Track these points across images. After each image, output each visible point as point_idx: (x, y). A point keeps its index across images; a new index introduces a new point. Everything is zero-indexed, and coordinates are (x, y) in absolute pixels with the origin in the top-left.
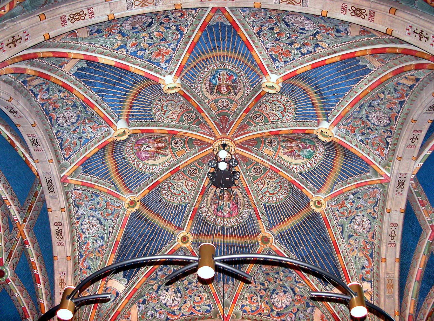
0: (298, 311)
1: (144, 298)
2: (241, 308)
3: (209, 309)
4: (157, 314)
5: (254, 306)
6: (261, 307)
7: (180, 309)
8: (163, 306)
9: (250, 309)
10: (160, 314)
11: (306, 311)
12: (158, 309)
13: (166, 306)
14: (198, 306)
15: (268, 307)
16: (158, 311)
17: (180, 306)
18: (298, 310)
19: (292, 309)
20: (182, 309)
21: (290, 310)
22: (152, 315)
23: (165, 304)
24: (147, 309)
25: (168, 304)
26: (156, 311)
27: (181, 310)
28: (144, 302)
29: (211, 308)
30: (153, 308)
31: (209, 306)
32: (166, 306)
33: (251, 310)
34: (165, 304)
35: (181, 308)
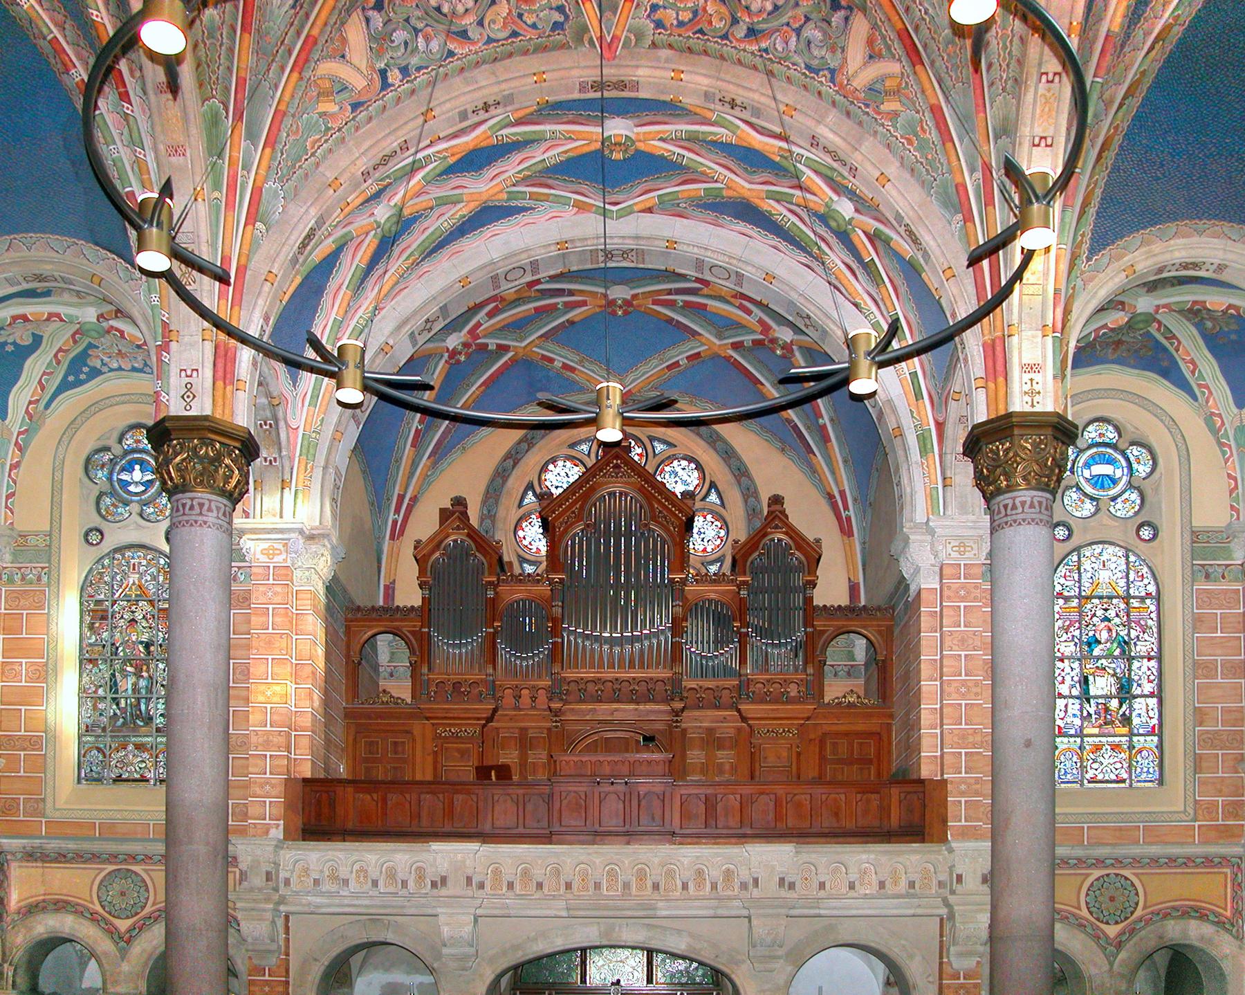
0: (805, 23)
2: (649, 16)
3: (562, 19)
4: (419, 40)
5: (685, 9)
6: (704, 10)
7: (480, 23)
8: (434, 14)
9: (675, 15)
10: (427, 39)
11: (829, 23)
12: (420, 25)
13: (441, 13)
14: (530, 12)
15: (723, 9)
16: (421, 30)
17: (479, 13)
18: (807, 19)
19: (790, 18)
20: (486, 23)
21: (784, 20)
22: (406, 43)
23: (438, 9)
24: (391, 27)
26: (416, 31)
27: (482, 26)
29: (567, 17)
30: (407, 20)
31: (560, 9)
32: (441, 13)
33: (677, 19)
35: (482, 18)
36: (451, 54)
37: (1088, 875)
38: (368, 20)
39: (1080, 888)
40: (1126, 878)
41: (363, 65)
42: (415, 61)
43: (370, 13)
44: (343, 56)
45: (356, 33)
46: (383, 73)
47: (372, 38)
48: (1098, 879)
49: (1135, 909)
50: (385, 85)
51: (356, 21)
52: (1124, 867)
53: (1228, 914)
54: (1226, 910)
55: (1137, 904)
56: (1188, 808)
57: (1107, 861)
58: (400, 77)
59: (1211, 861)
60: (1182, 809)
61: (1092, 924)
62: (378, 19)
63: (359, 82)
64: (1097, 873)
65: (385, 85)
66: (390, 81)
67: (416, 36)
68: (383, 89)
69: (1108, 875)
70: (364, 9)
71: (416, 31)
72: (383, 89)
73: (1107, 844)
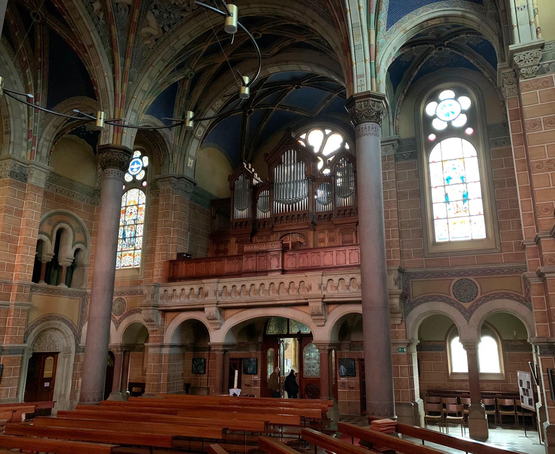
1: (154, 3)
7: (189, 5)
10: (174, 15)
12: (171, 10)
22: (168, 17)
23: (175, 4)
25: (177, 4)
26: (170, 13)
27: (190, 6)
28: (156, 7)
30: (166, 10)
34: (175, 4)
36: (182, 17)
37: (453, 280)
38: (153, 13)
39: (450, 285)
40: (471, 281)
41: (156, 27)
42: (172, 22)
43: (153, 11)
44: (149, 26)
45: (150, 17)
46: (163, 28)
47: (156, 18)
48: (457, 282)
49: (477, 295)
50: (164, 32)
51: (149, 13)
52: (469, 276)
53: (524, 296)
54: (522, 294)
55: (477, 292)
56: (497, 247)
57: (461, 273)
58: (168, 28)
59: (512, 271)
60: (495, 247)
61: (457, 302)
62: (157, 12)
63: (155, 32)
64: (457, 279)
65: (164, 32)
66: (165, 30)
67: (170, 14)
68: (163, 33)
69: (462, 279)
70: (151, 10)
71: (170, 13)
72: (163, 33)
73: (460, 265)
